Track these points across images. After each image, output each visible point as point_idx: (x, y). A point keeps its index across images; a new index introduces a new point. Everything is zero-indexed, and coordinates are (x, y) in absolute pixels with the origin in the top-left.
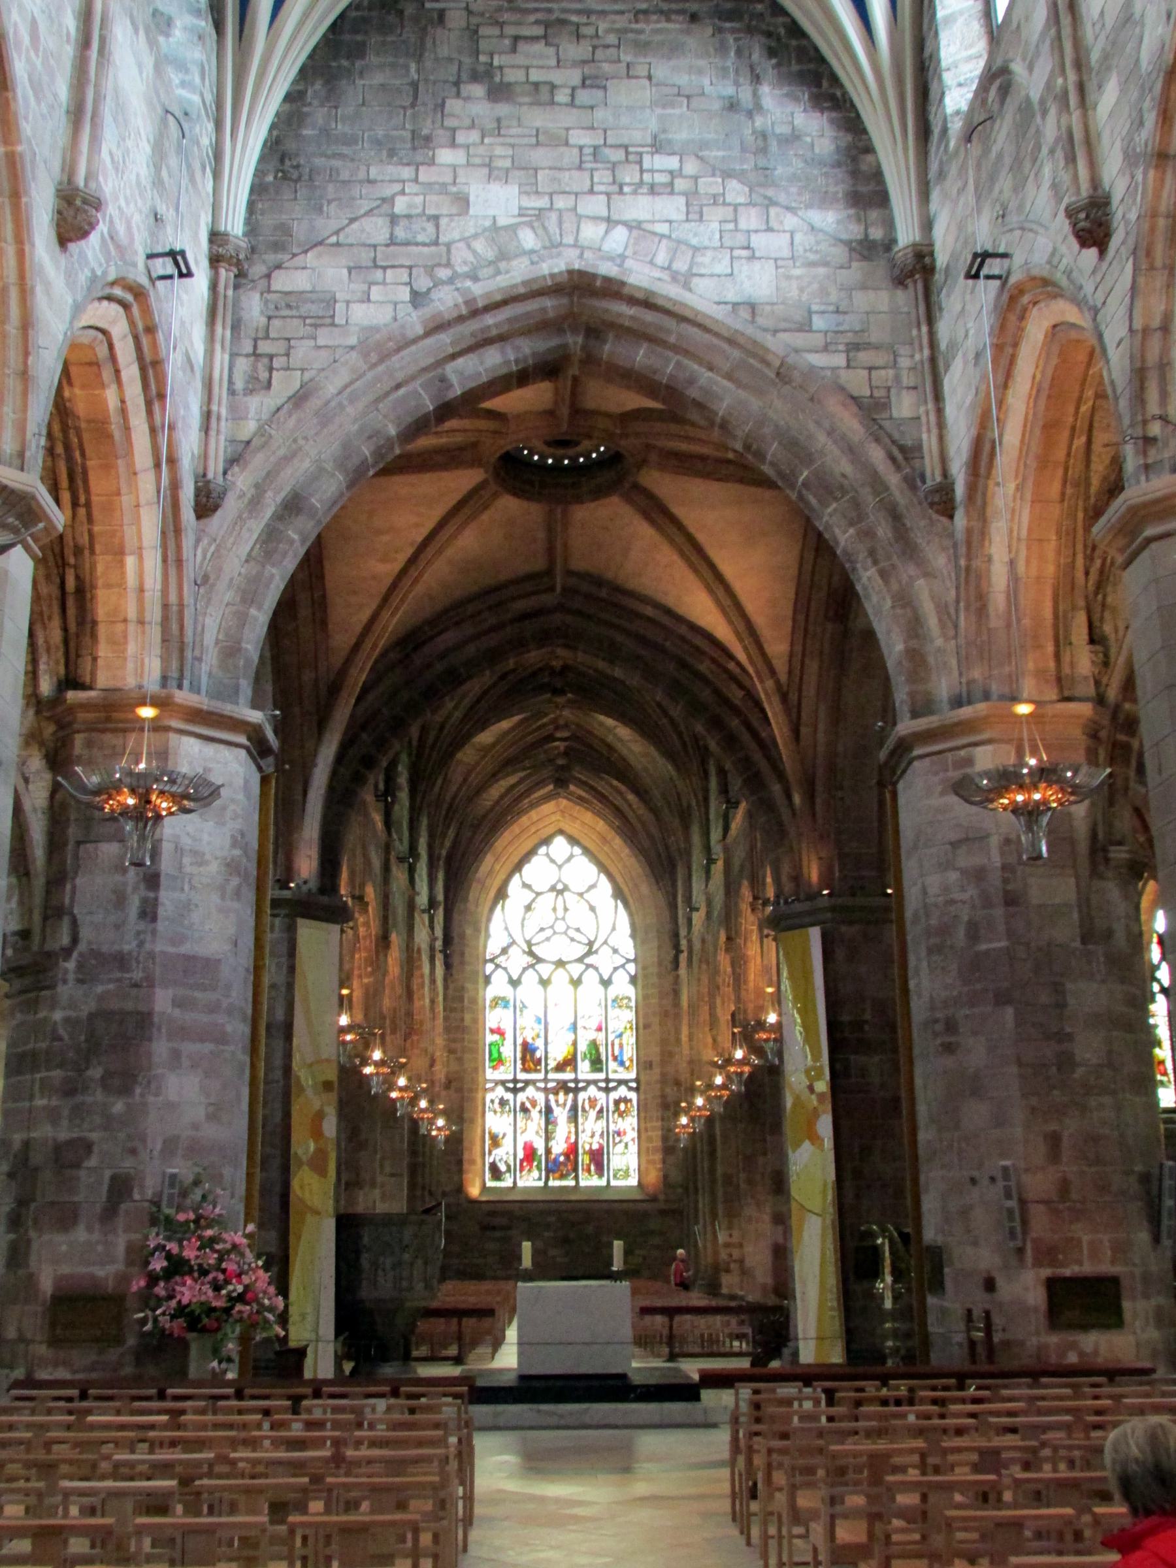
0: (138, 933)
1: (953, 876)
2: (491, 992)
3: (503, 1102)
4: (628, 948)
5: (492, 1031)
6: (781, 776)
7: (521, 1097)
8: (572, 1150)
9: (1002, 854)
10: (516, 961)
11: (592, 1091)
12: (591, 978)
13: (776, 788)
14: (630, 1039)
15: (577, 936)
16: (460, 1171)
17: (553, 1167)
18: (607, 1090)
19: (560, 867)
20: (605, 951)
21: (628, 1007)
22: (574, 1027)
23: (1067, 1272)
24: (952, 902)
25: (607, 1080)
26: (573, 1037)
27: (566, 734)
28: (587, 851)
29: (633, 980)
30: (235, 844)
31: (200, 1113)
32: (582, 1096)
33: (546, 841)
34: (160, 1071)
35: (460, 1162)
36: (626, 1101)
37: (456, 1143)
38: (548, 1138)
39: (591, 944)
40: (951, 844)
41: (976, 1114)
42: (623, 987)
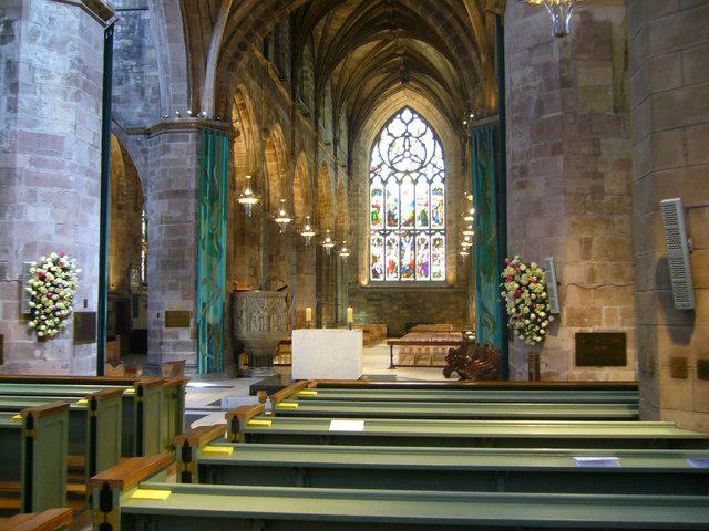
0: (7, 120)
1: (530, 70)
2: (373, 187)
3: (379, 241)
4: (441, 164)
5: (373, 206)
6: (475, 45)
7: (388, 238)
8: (413, 266)
9: (561, 51)
10: (385, 171)
11: (423, 235)
12: (422, 178)
13: (473, 53)
14: (442, 210)
15: (416, 159)
16: (357, 273)
17: (403, 271)
18: (430, 235)
19: (407, 124)
20: (430, 166)
21: (441, 194)
22: (414, 203)
23: (590, 330)
24: (528, 88)
25: (430, 230)
26: (412, 209)
27: (402, 52)
28: (420, 116)
29: (443, 180)
30: (73, 66)
31: (52, 229)
32: (418, 237)
33: (401, 112)
34: (21, 203)
35: (357, 269)
36: (439, 240)
37: (354, 261)
38: (401, 257)
39: (423, 162)
40: (529, 48)
41: (536, 227)
42: (438, 183)
